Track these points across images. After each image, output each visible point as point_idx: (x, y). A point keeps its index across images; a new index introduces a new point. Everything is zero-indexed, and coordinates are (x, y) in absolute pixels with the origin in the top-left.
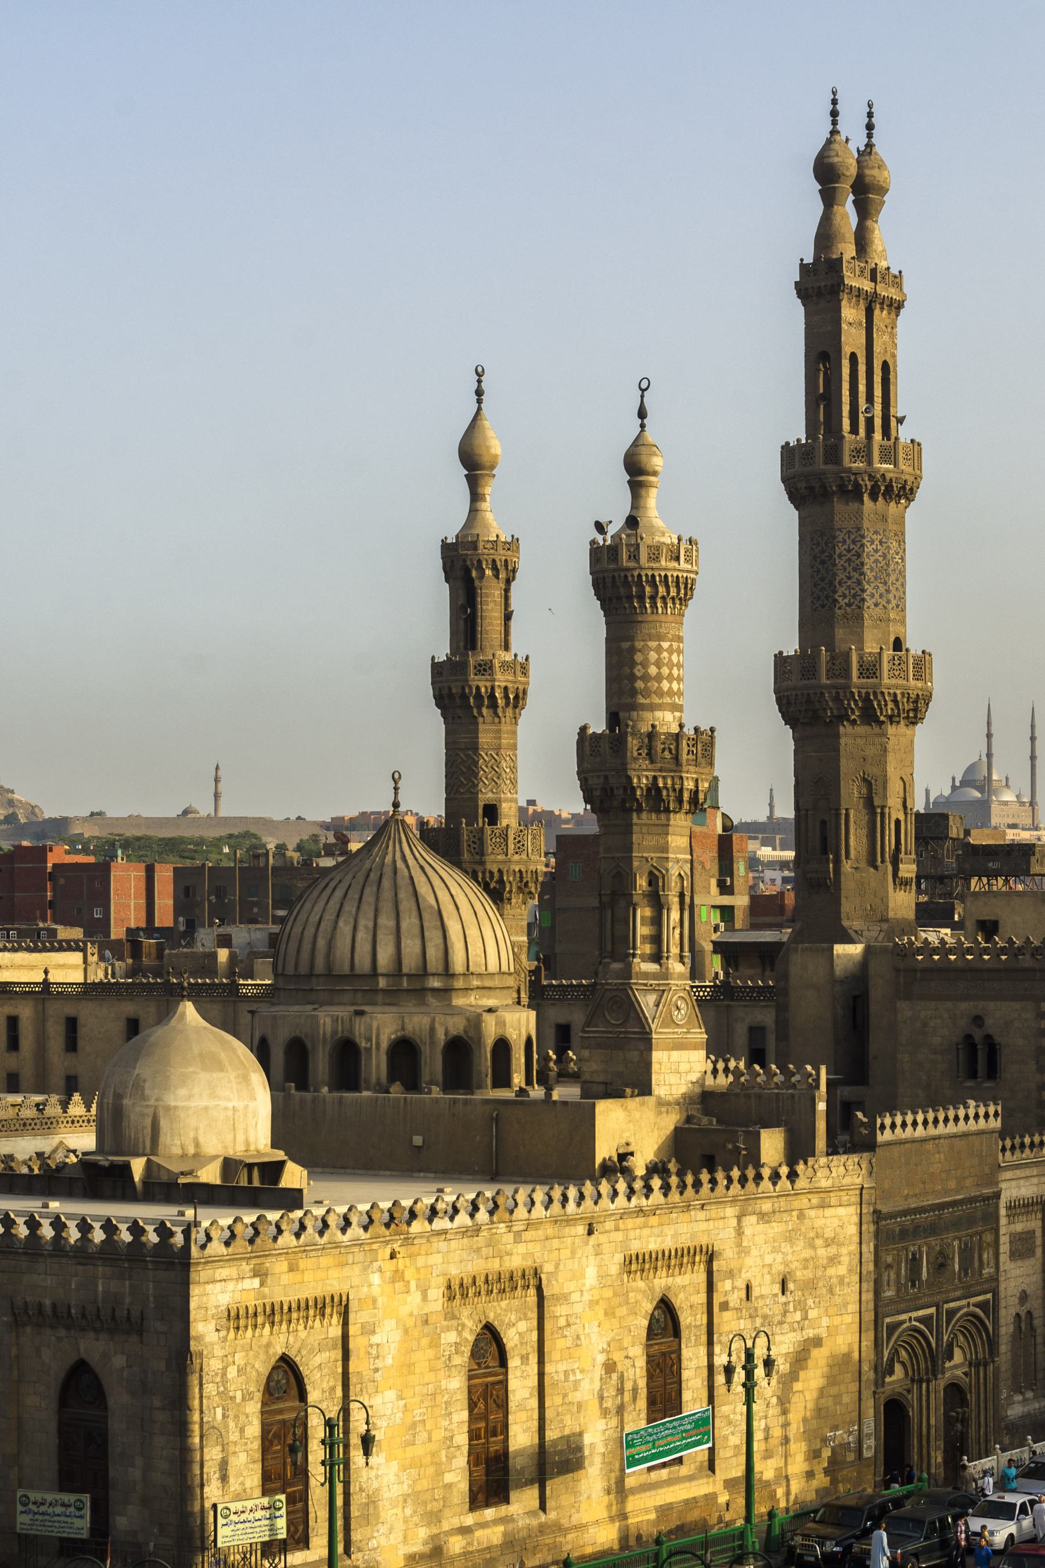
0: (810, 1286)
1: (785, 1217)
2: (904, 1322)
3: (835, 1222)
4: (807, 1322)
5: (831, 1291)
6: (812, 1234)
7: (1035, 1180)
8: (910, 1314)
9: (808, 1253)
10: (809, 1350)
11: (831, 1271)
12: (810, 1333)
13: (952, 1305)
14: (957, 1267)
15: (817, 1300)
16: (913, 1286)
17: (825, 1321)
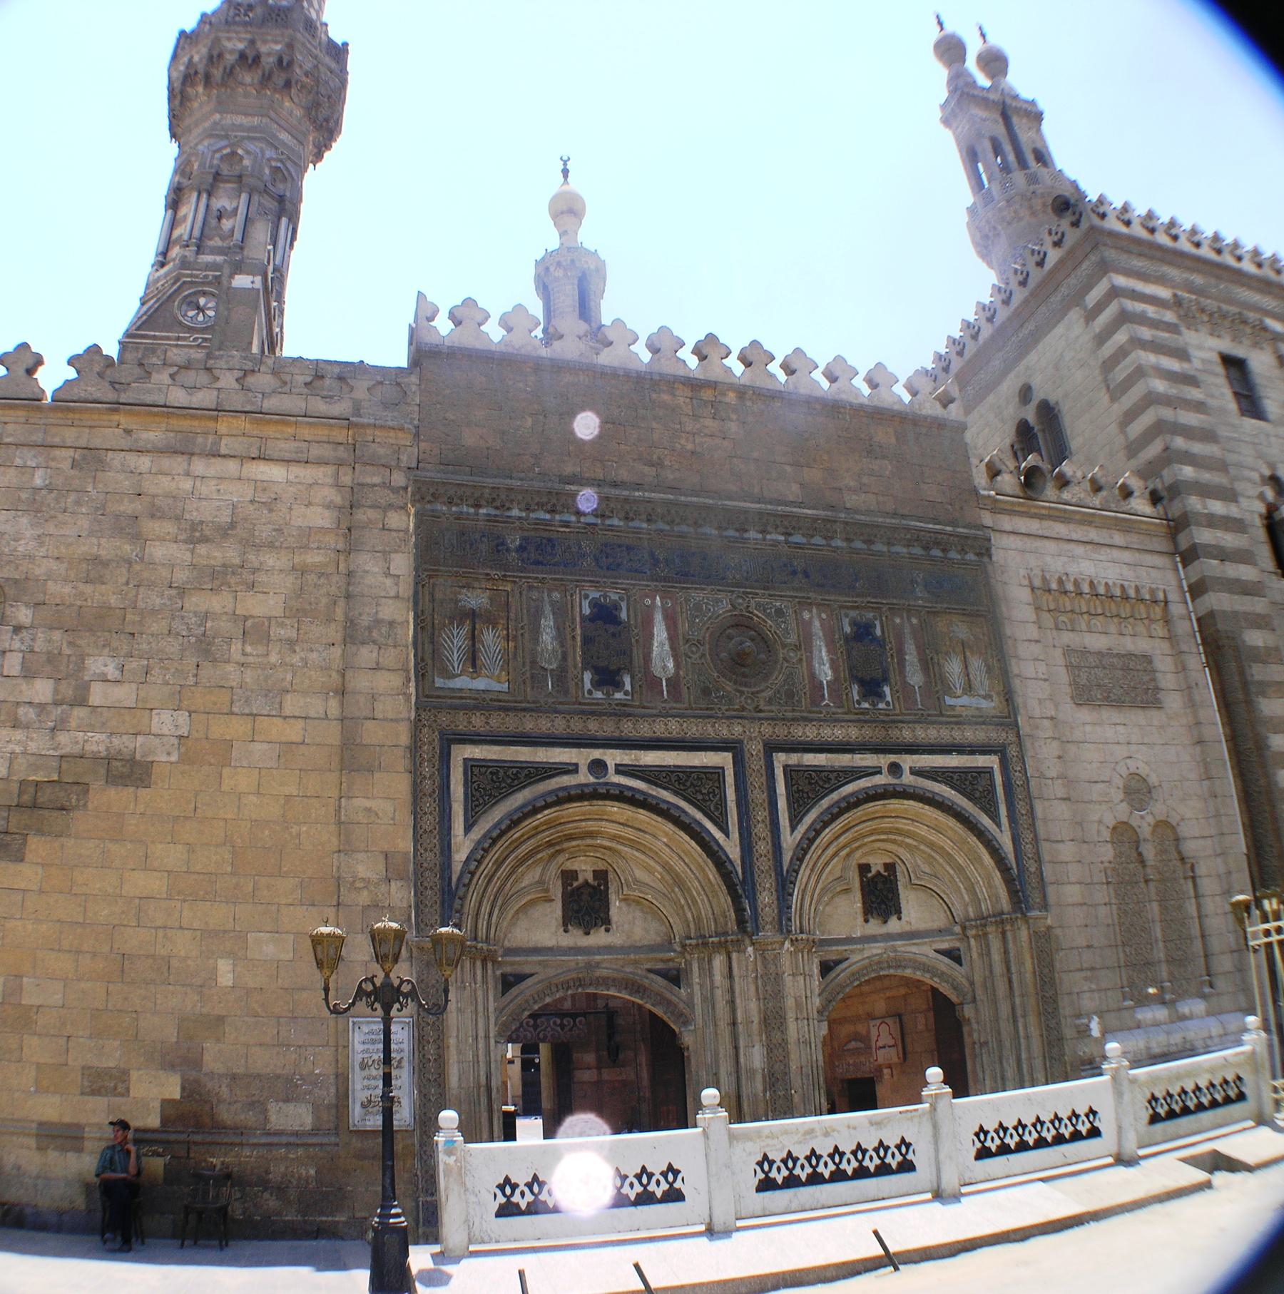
0: (88, 624)
1: (29, 458)
2: (572, 769)
3: (238, 493)
4: (79, 713)
5: (206, 648)
6: (128, 507)
7: (1126, 556)
8: (596, 754)
9: (108, 547)
10: (83, 787)
11: (218, 603)
12: (97, 742)
13: (811, 759)
14: (825, 673)
15: (133, 664)
16: (607, 679)
17: (166, 722)
